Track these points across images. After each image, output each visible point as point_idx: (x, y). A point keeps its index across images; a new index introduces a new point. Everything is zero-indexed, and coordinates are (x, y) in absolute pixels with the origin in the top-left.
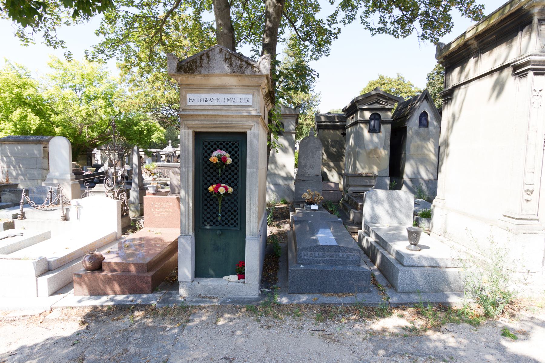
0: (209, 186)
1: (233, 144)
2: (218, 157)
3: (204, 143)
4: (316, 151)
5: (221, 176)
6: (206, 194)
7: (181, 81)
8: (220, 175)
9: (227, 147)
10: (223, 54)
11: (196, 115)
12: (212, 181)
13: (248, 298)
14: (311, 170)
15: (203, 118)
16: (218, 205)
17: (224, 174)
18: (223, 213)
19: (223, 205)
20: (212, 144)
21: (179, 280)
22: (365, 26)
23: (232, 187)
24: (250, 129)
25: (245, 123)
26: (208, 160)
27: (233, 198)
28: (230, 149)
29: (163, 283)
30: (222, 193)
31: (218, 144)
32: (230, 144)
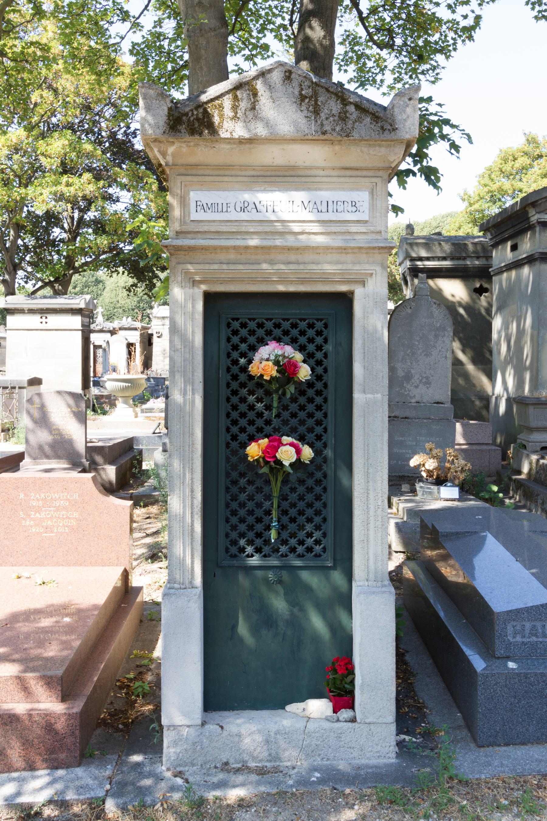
0: (244, 446)
1: (311, 326)
2: (276, 363)
3: (229, 325)
4: (436, 336)
5: (278, 416)
6: (234, 467)
7: (174, 155)
8: (274, 411)
9: (295, 332)
10: (295, 83)
11: (215, 249)
12: (251, 429)
13: (367, 766)
14: (423, 389)
15: (232, 256)
16: (268, 497)
17: (285, 408)
18: (285, 520)
19: (284, 498)
20: (252, 325)
21: (164, 721)
22: (535, 13)
23: (311, 446)
24: (363, 283)
25: (350, 266)
26: (244, 369)
27: (311, 475)
28: (303, 340)
29: (98, 731)
30: (286, 463)
31: (269, 325)
32: (303, 325)
